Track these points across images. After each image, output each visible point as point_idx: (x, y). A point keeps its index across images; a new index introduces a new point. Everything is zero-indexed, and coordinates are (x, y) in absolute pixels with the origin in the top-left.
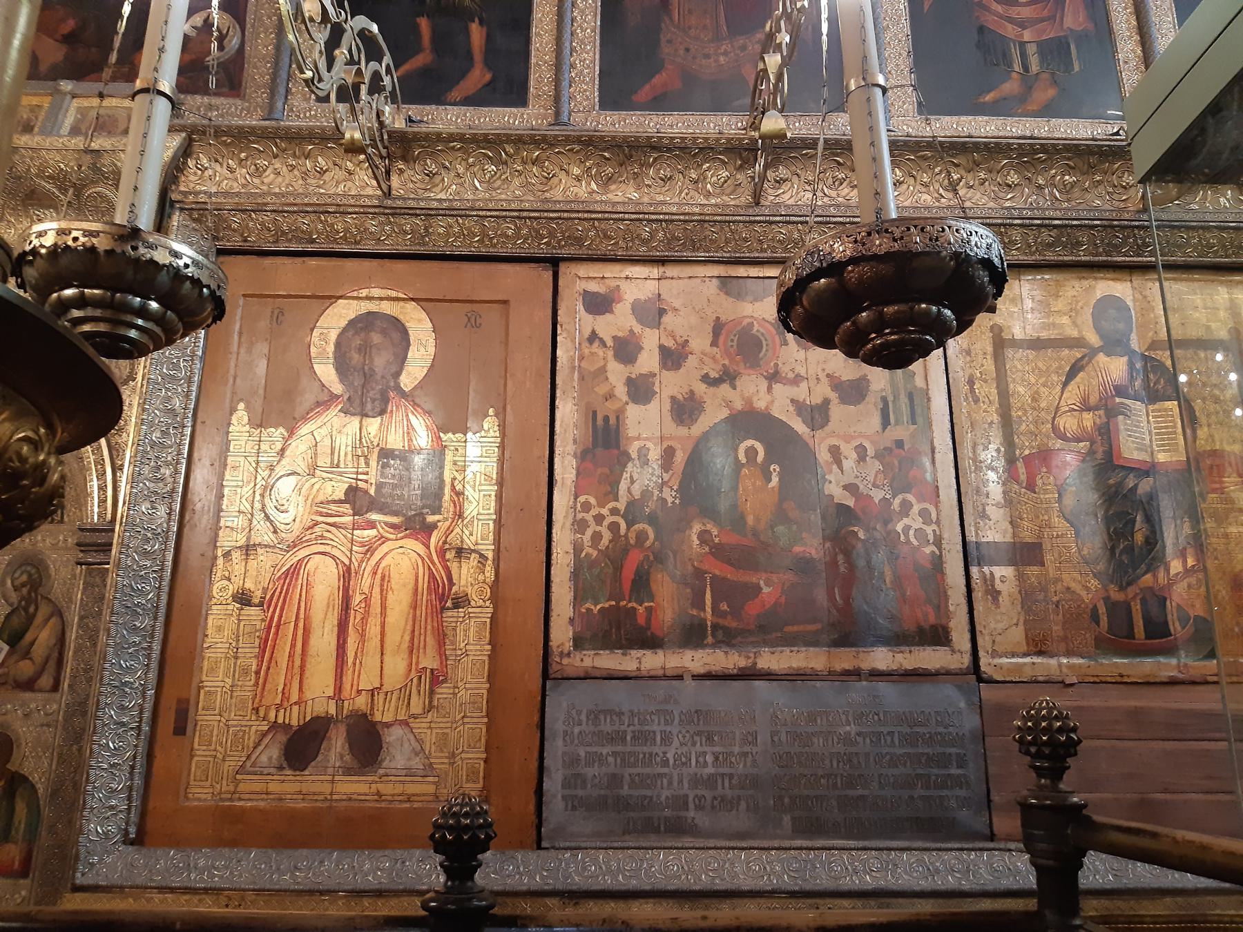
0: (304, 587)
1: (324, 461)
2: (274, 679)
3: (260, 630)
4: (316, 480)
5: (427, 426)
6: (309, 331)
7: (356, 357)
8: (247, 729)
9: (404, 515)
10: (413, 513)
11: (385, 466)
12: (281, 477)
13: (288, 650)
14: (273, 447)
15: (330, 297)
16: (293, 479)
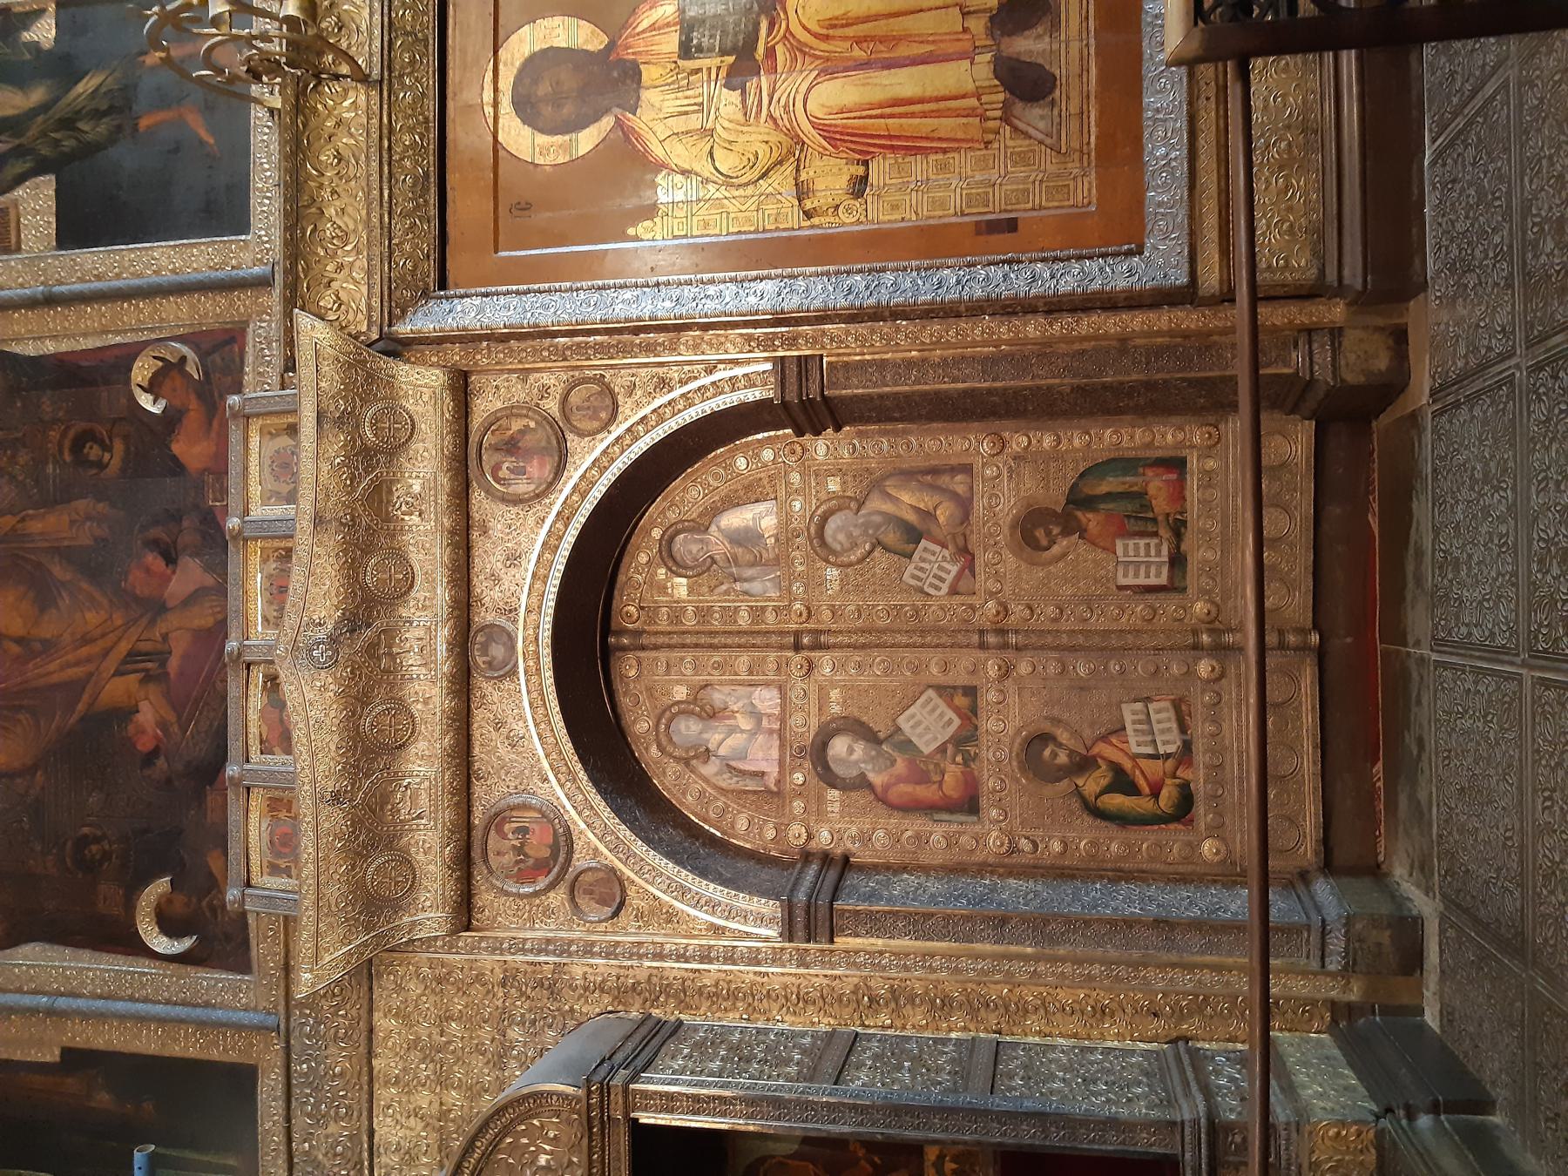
0: (845, 115)
1: (695, 122)
2: (952, 129)
3: (896, 159)
4: (718, 126)
5: (651, 8)
6: (539, 169)
7: (568, 110)
8: (1009, 151)
9: (758, 15)
10: (755, 5)
11: (700, 49)
12: (716, 169)
13: (917, 121)
14: (679, 185)
15: (496, 151)
16: (718, 153)
